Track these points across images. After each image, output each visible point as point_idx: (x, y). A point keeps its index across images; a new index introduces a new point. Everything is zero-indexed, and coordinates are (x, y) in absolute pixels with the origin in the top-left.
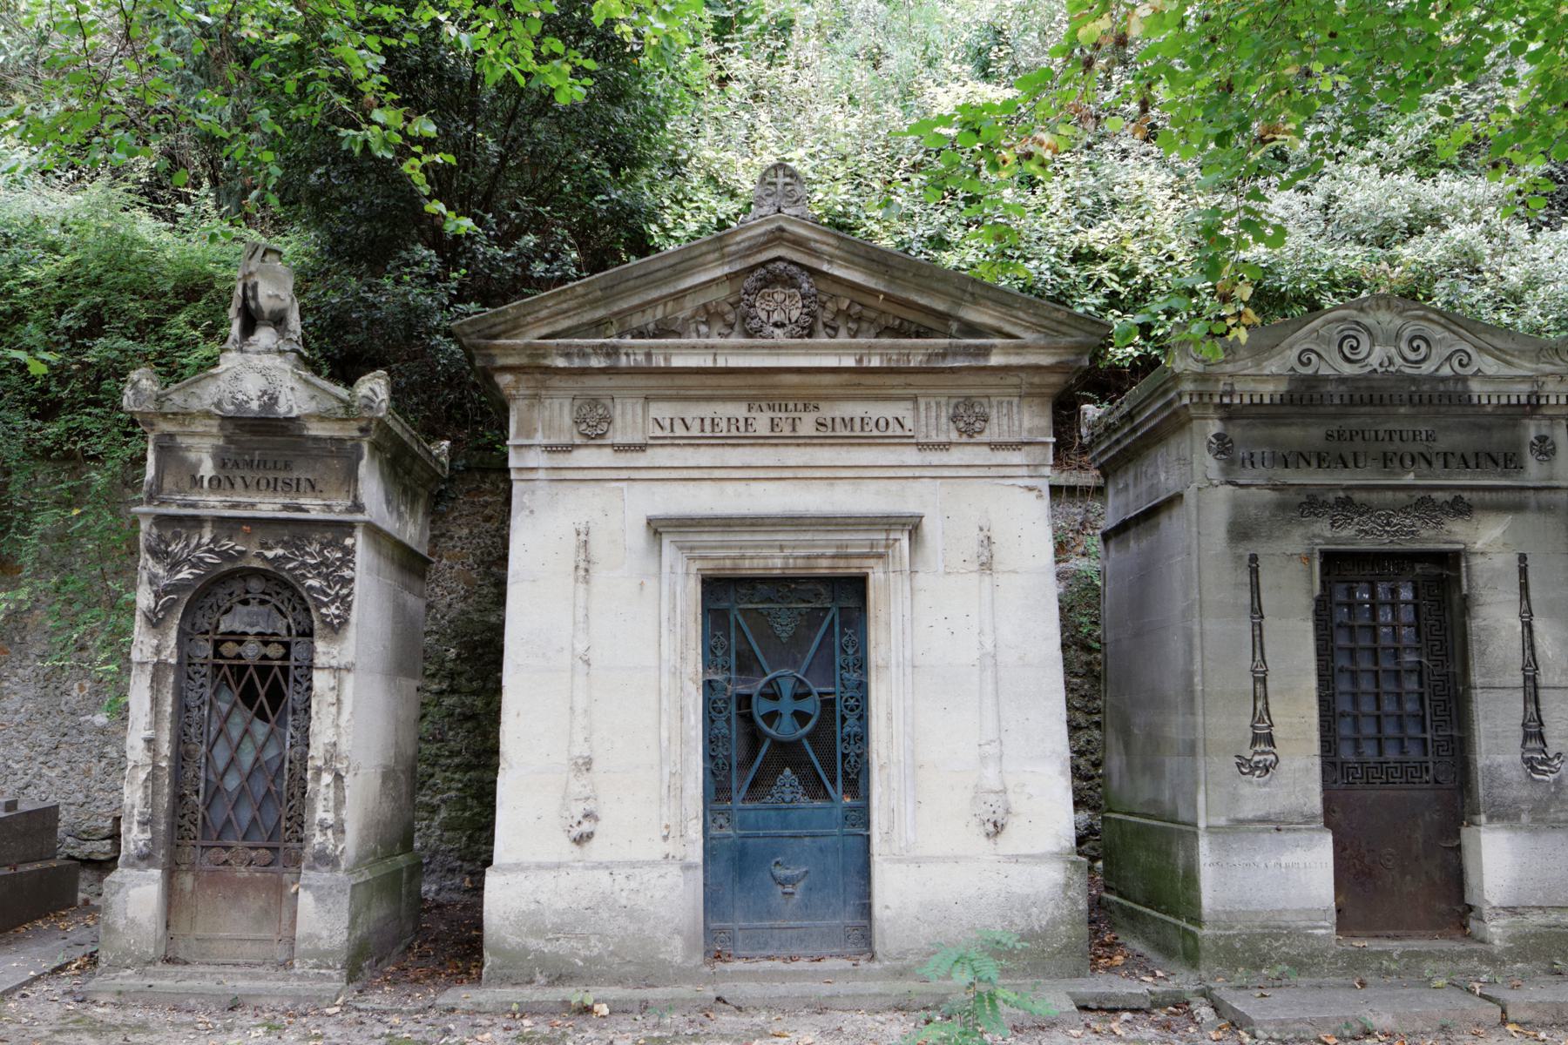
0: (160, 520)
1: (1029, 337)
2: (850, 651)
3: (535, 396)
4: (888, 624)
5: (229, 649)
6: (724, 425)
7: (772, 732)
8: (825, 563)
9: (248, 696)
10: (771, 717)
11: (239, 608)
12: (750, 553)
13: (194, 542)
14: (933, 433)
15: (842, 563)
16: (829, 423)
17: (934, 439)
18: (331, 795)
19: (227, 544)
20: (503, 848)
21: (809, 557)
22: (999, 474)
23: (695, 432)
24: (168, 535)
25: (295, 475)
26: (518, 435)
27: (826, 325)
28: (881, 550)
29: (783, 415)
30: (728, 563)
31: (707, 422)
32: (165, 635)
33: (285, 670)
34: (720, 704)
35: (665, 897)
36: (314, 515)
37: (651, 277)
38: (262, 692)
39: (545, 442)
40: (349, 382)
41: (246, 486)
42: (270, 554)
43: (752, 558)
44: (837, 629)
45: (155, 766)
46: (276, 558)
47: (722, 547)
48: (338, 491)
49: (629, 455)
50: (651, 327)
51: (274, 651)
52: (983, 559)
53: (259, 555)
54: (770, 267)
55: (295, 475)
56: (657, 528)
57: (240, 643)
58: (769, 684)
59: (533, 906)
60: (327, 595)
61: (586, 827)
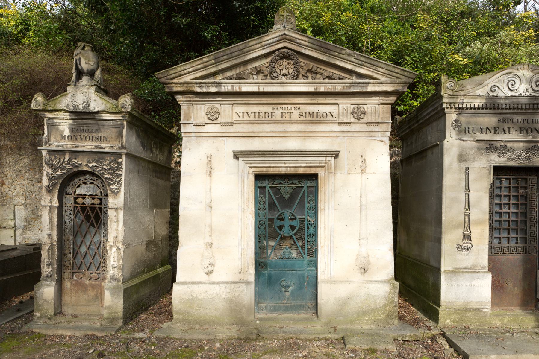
0: (49, 151)
1: (384, 79)
2: (311, 203)
3: (191, 104)
4: (325, 193)
5: (80, 200)
6: (263, 115)
7: (281, 233)
8: (301, 169)
9: (88, 218)
10: (281, 228)
11: (83, 185)
12: (273, 165)
13: (62, 160)
14: (345, 119)
15: (308, 169)
16: (304, 114)
17: (345, 121)
18: (116, 255)
19: (74, 161)
20: (180, 276)
21: (295, 167)
22: (370, 135)
23: (252, 118)
24: (53, 158)
25: (100, 135)
26: (184, 120)
27: (303, 76)
29: (286, 112)
30: (264, 169)
31: (257, 114)
32: (53, 195)
33: (100, 209)
34: (262, 222)
35: (239, 295)
36: (107, 150)
37: (233, 55)
38: (92, 217)
39: (194, 122)
40: (116, 97)
41: (82, 139)
42: (90, 165)
43: (273, 167)
44: (306, 195)
45: (52, 244)
46: (93, 167)
47: (262, 163)
48: (116, 141)
49: (227, 127)
50: (235, 76)
51: (96, 201)
52: (363, 168)
53: (87, 165)
54: (281, 50)
55: (100, 135)
56: (236, 156)
57: (84, 198)
58: (280, 215)
59: (190, 298)
60: (112, 181)
61: (210, 269)
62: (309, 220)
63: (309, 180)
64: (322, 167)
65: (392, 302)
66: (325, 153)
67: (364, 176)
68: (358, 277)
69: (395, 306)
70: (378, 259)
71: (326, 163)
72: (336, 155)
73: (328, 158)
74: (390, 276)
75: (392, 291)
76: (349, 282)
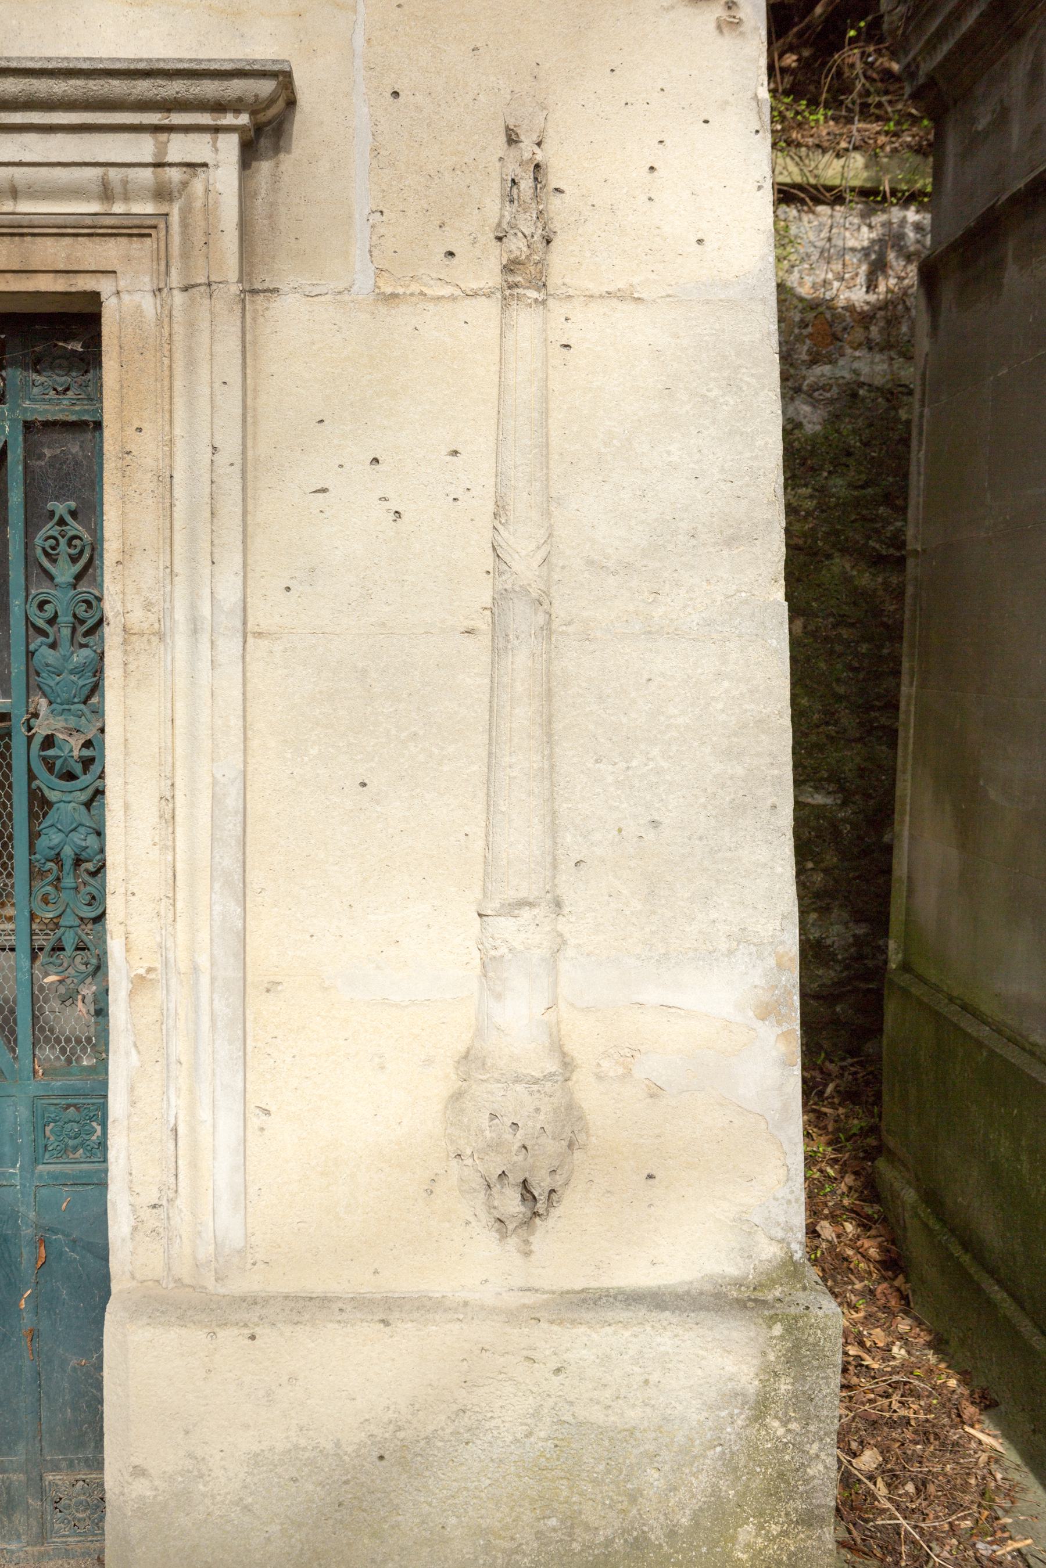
28: (146, 207)
52: (517, 246)
62: (41, 729)
63: (36, 364)
64: (137, 230)
65: (782, 1483)
66: (143, 88)
67: (526, 321)
68: (478, 1265)
69: (808, 1520)
70: (655, 1092)
71: (162, 193)
72: (266, 118)
73: (181, 148)
74: (769, 1252)
75: (784, 1386)
76: (386, 1309)
